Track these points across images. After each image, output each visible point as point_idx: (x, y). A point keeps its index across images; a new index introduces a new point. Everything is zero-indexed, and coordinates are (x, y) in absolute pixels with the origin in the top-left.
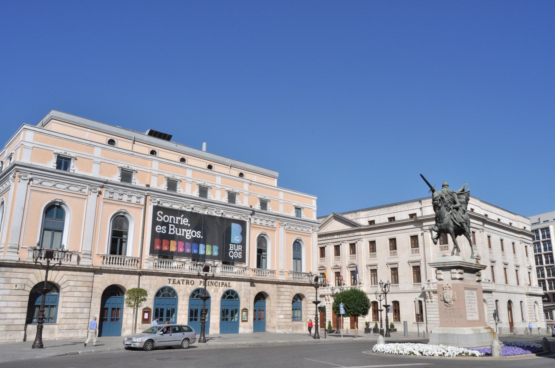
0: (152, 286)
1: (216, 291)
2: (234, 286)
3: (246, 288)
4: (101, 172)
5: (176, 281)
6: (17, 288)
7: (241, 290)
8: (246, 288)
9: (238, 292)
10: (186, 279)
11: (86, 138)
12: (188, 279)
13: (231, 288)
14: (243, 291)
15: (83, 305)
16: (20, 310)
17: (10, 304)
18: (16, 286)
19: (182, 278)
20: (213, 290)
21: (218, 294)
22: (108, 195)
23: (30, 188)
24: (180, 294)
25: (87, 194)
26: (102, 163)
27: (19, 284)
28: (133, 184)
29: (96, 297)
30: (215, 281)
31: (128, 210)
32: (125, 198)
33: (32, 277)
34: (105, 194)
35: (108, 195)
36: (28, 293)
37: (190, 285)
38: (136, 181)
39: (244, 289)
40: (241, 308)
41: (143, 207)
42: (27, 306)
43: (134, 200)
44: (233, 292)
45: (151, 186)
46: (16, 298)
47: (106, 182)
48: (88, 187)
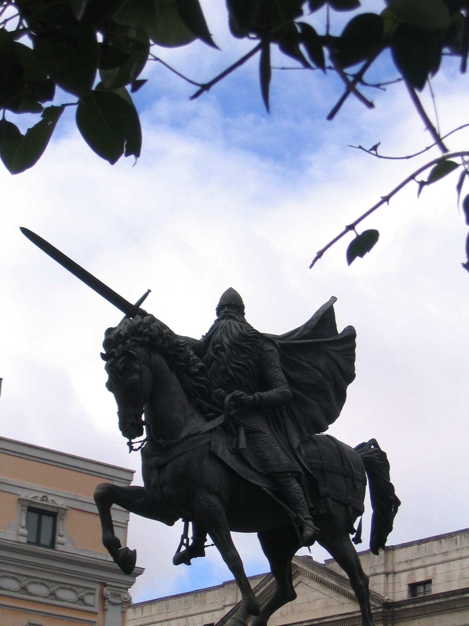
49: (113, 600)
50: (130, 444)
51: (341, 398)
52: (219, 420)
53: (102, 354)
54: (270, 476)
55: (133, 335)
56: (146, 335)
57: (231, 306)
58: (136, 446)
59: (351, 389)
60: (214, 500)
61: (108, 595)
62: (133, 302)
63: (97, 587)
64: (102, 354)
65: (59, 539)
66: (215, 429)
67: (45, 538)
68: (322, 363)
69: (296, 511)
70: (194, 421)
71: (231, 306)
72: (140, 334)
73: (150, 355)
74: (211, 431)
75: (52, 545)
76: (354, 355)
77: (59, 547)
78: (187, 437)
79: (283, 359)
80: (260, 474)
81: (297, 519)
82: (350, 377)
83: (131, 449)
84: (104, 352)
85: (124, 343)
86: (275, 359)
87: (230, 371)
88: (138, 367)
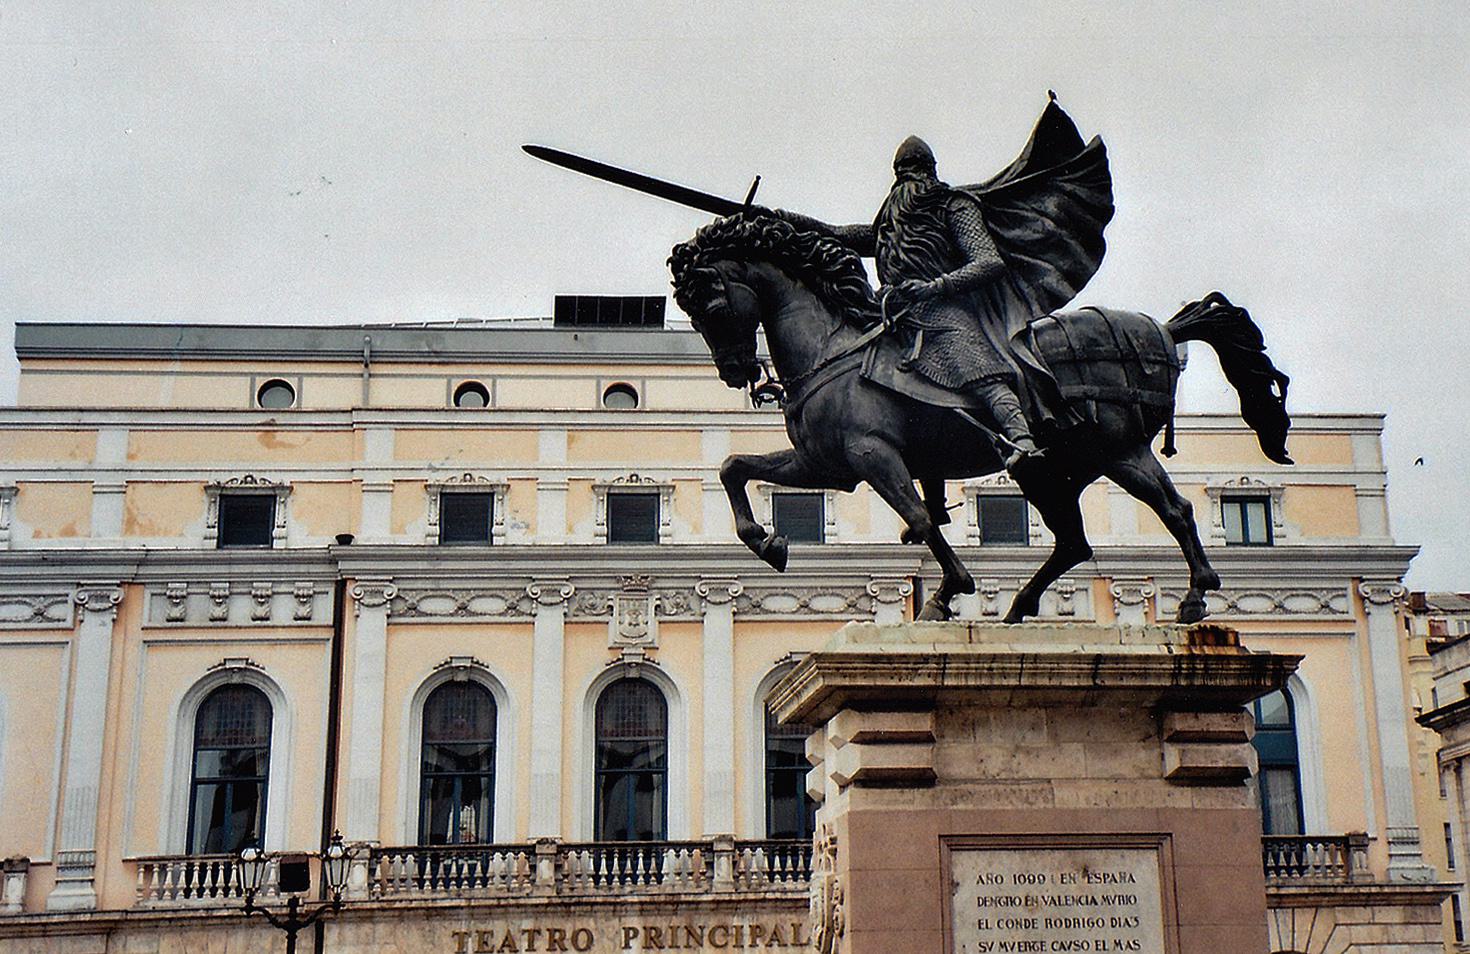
4: (130, 524)
10: (546, 923)
12: (557, 924)
19: (528, 924)
22: (162, 611)
28: (277, 544)
30: (712, 922)
31: (260, 656)
32: (242, 610)
34: (146, 608)
38: (299, 528)
41: (330, 634)
43: (284, 610)
45: (359, 539)
47: (145, 559)
49: (1376, 599)
52: (880, 329)
53: (672, 283)
54: (966, 390)
56: (730, 240)
60: (869, 443)
61: (1367, 593)
63: (1350, 585)
64: (672, 283)
65: (1276, 531)
66: (872, 343)
67: (1257, 532)
70: (840, 340)
72: (714, 243)
73: (745, 268)
74: (862, 349)
75: (1270, 543)
77: (1277, 542)
78: (823, 366)
84: (674, 280)
88: (723, 288)
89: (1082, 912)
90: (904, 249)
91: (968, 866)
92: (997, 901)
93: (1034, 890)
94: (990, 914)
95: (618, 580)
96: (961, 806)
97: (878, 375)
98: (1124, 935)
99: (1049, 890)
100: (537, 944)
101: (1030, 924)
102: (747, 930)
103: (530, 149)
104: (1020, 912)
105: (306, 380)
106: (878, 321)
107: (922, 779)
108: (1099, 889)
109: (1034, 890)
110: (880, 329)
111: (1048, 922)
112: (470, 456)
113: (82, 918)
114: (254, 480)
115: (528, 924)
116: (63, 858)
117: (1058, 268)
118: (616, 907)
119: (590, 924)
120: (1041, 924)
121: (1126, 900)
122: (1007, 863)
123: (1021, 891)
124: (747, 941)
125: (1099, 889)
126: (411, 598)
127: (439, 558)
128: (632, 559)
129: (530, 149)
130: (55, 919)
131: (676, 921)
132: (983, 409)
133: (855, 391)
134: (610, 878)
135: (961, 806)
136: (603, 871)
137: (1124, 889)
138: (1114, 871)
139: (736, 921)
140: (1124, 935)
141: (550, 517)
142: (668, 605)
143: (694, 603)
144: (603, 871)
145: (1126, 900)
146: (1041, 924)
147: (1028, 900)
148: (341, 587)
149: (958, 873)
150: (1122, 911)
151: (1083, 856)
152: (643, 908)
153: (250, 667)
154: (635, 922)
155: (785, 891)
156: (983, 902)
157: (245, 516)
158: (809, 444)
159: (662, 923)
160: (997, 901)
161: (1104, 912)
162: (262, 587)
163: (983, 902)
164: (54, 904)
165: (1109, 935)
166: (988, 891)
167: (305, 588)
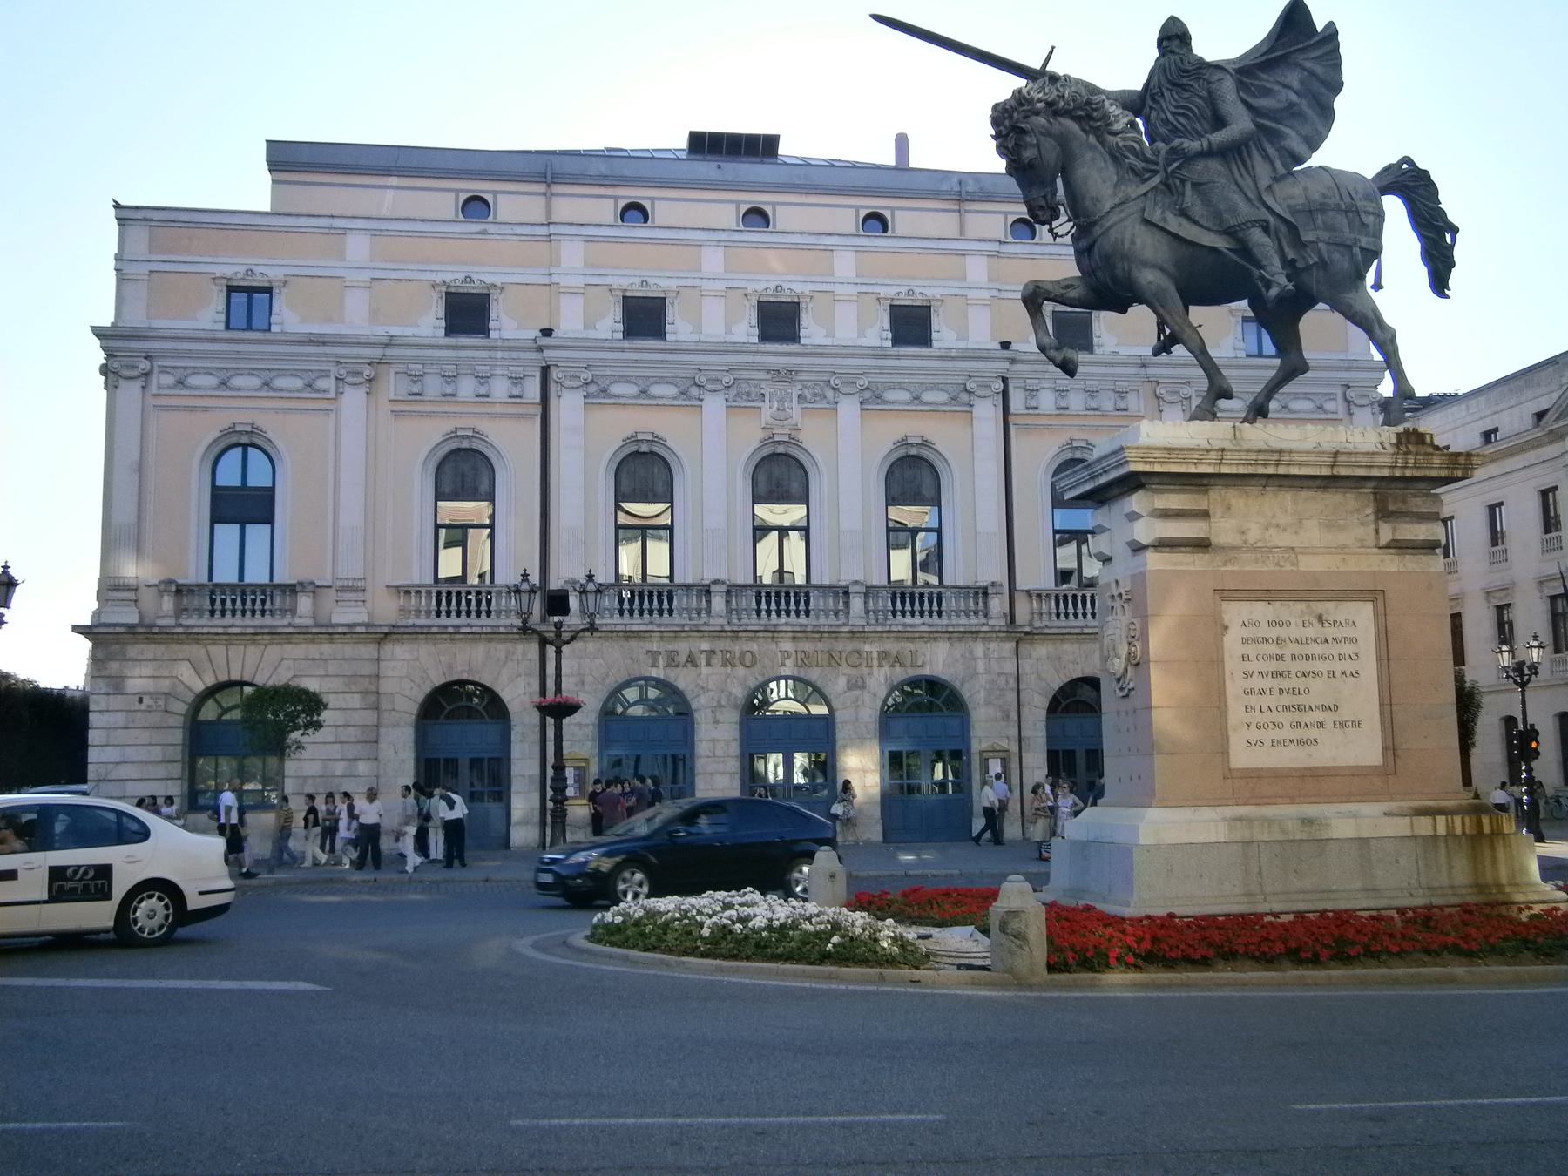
0: (589, 679)
1: (857, 685)
2: (938, 660)
3: (995, 667)
4: (375, 315)
5: (682, 658)
6: (143, 707)
7: (974, 675)
8: (995, 667)
9: (957, 684)
11: (382, 215)
13: (927, 671)
14: (983, 679)
15: (353, 751)
16: (161, 771)
17: (131, 753)
18: (141, 700)
20: (842, 682)
21: (867, 697)
22: (403, 387)
23: (152, 401)
24: (701, 704)
25: (332, 395)
26: (375, 283)
27: (148, 693)
29: (396, 725)
31: (484, 426)
33: (185, 673)
34: (393, 386)
35: (403, 387)
36: (179, 721)
37: (741, 671)
39: (988, 671)
40: (976, 746)
41: (538, 410)
42: (179, 758)
43: (500, 389)
44: (934, 686)
46: (145, 736)
48: (333, 369)
50: (1051, 230)
51: (1327, 115)
55: (1021, 105)
57: (1174, 37)
58: (1061, 231)
59: (1339, 103)
62: (1037, 65)
66: (1154, 188)
68: (1294, 78)
69: (1260, 266)
71: (1174, 37)
76: (1339, 57)
79: (1241, 86)
80: (1216, 232)
81: (1262, 278)
82: (1337, 87)
83: (1055, 236)
85: (1011, 117)
86: (1228, 89)
87: (1170, 117)
89: (1318, 649)
90: (1174, 114)
91: (1236, 613)
92: (1256, 641)
93: (1282, 632)
94: (1249, 650)
95: (768, 371)
96: (1229, 568)
97: (1156, 216)
98: (1348, 666)
99: (1295, 632)
100: (713, 662)
101: (1279, 658)
102: (875, 655)
103: (876, 17)
104: (1273, 649)
105: (499, 196)
106: (1156, 172)
107: (1202, 545)
108: (1330, 632)
109: (1282, 632)
110: (1156, 180)
111: (1294, 657)
112: (640, 267)
113: (359, 629)
114: (472, 281)
115: (705, 646)
116: (340, 583)
117: (1299, 133)
118: (773, 632)
119: (754, 647)
120: (1288, 658)
121: (1349, 640)
122: (1261, 611)
123: (1274, 633)
124: (875, 663)
125: (1330, 632)
126: (603, 383)
127: (623, 350)
128: (778, 355)
129: (876, 17)
130: (340, 630)
131: (820, 646)
132: (1245, 250)
133: (1140, 229)
134: (769, 612)
135: (1229, 568)
136: (764, 606)
137: (1348, 632)
138: (1341, 618)
139: (867, 648)
140: (1348, 666)
141: (712, 319)
142: (807, 393)
143: (830, 393)
144: (764, 606)
145: (1349, 640)
146: (1288, 658)
147: (1279, 641)
148: (545, 371)
149: (1226, 619)
150: (1347, 649)
151: (1320, 607)
152: (798, 634)
153: (476, 434)
154: (787, 645)
155: (904, 625)
156: (1246, 641)
157: (467, 313)
158: (1099, 274)
159: (808, 646)
160: (1256, 641)
161: (1333, 649)
162: (483, 370)
163: (1246, 641)
164: (336, 619)
165: (1338, 666)
166: (1246, 633)
167: (517, 371)
